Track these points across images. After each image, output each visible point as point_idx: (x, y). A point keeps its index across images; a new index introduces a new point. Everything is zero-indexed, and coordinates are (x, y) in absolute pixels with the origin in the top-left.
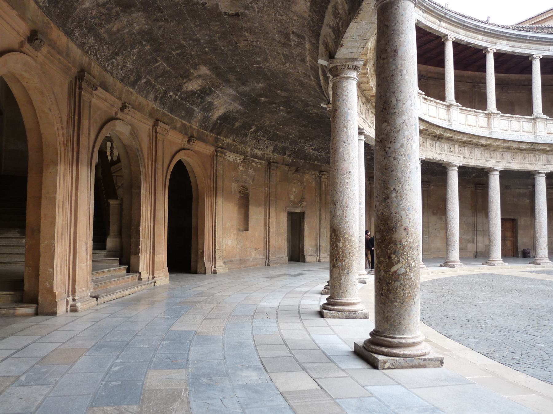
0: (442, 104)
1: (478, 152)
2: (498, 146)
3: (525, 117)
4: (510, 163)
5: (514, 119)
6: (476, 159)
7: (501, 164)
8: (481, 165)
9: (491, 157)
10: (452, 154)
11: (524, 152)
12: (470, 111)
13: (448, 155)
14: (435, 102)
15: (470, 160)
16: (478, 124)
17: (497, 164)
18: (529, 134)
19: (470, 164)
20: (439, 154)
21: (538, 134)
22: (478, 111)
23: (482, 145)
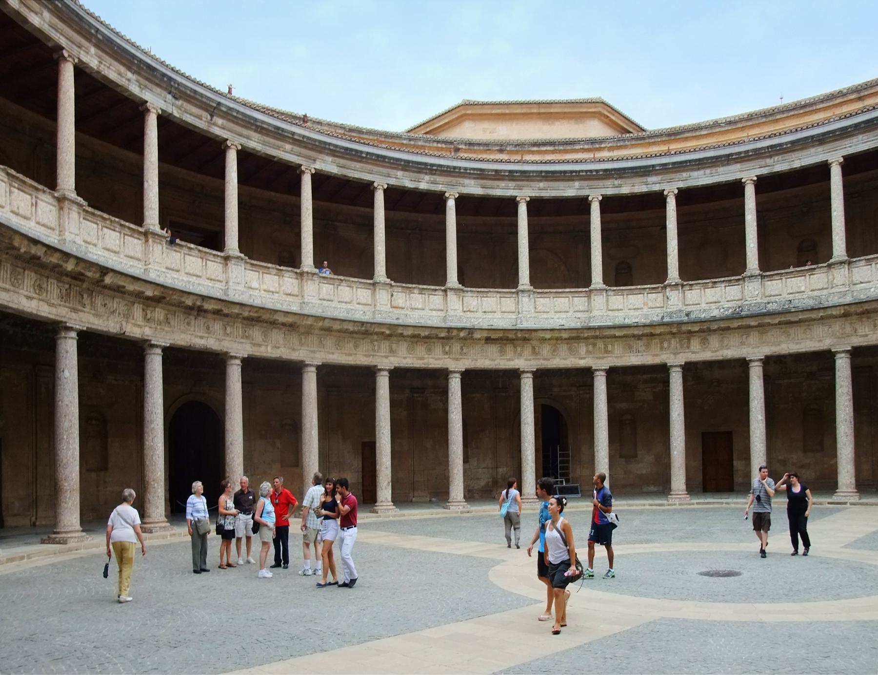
0: (214, 255)
1: (277, 336)
2: (311, 325)
3: (362, 281)
4: (333, 353)
5: (344, 284)
6: (275, 347)
7: (317, 355)
8: (285, 357)
9: (301, 344)
10: (228, 338)
11: (355, 335)
12: (269, 268)
13: (220, 341)
14: (199, 251)
15: (263, 349)
16: (283, 288)
17: (312, 355)
18: (366, 308)
19: (265, 355)
20: (201, 337)
21: (377, 308)
22: (282, 268)
23: (284, 324)
